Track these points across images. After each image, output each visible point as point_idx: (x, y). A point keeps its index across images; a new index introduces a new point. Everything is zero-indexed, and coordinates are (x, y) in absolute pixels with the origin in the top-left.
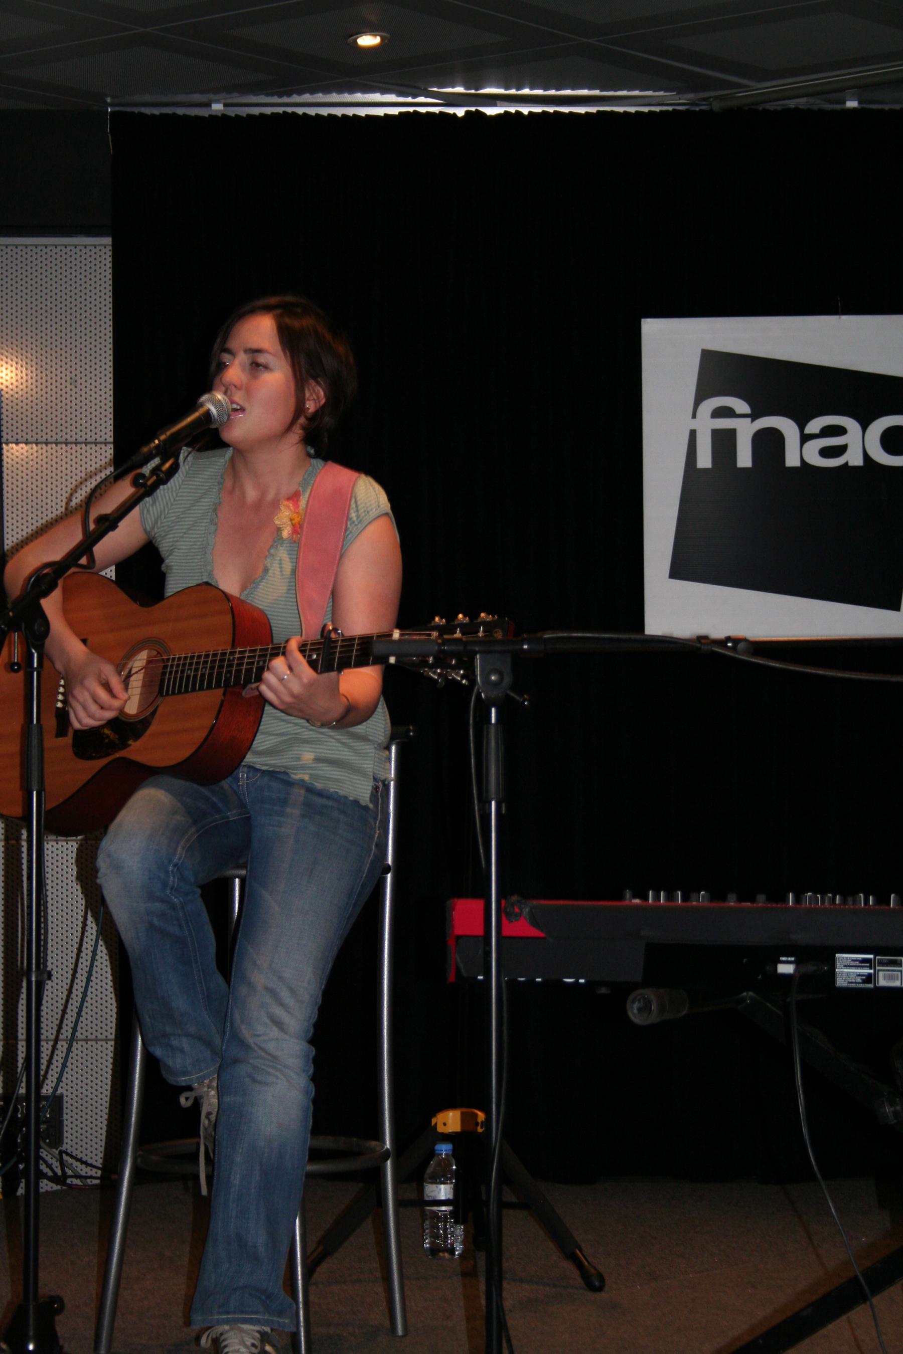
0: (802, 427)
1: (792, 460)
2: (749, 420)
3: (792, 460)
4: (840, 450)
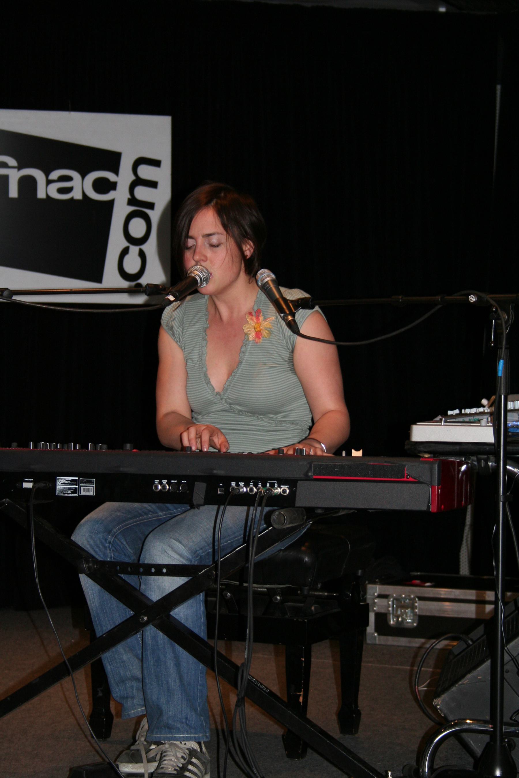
0: (47, 175)
1: (41, 194)
2: (16, 170)
3: (41, 194)
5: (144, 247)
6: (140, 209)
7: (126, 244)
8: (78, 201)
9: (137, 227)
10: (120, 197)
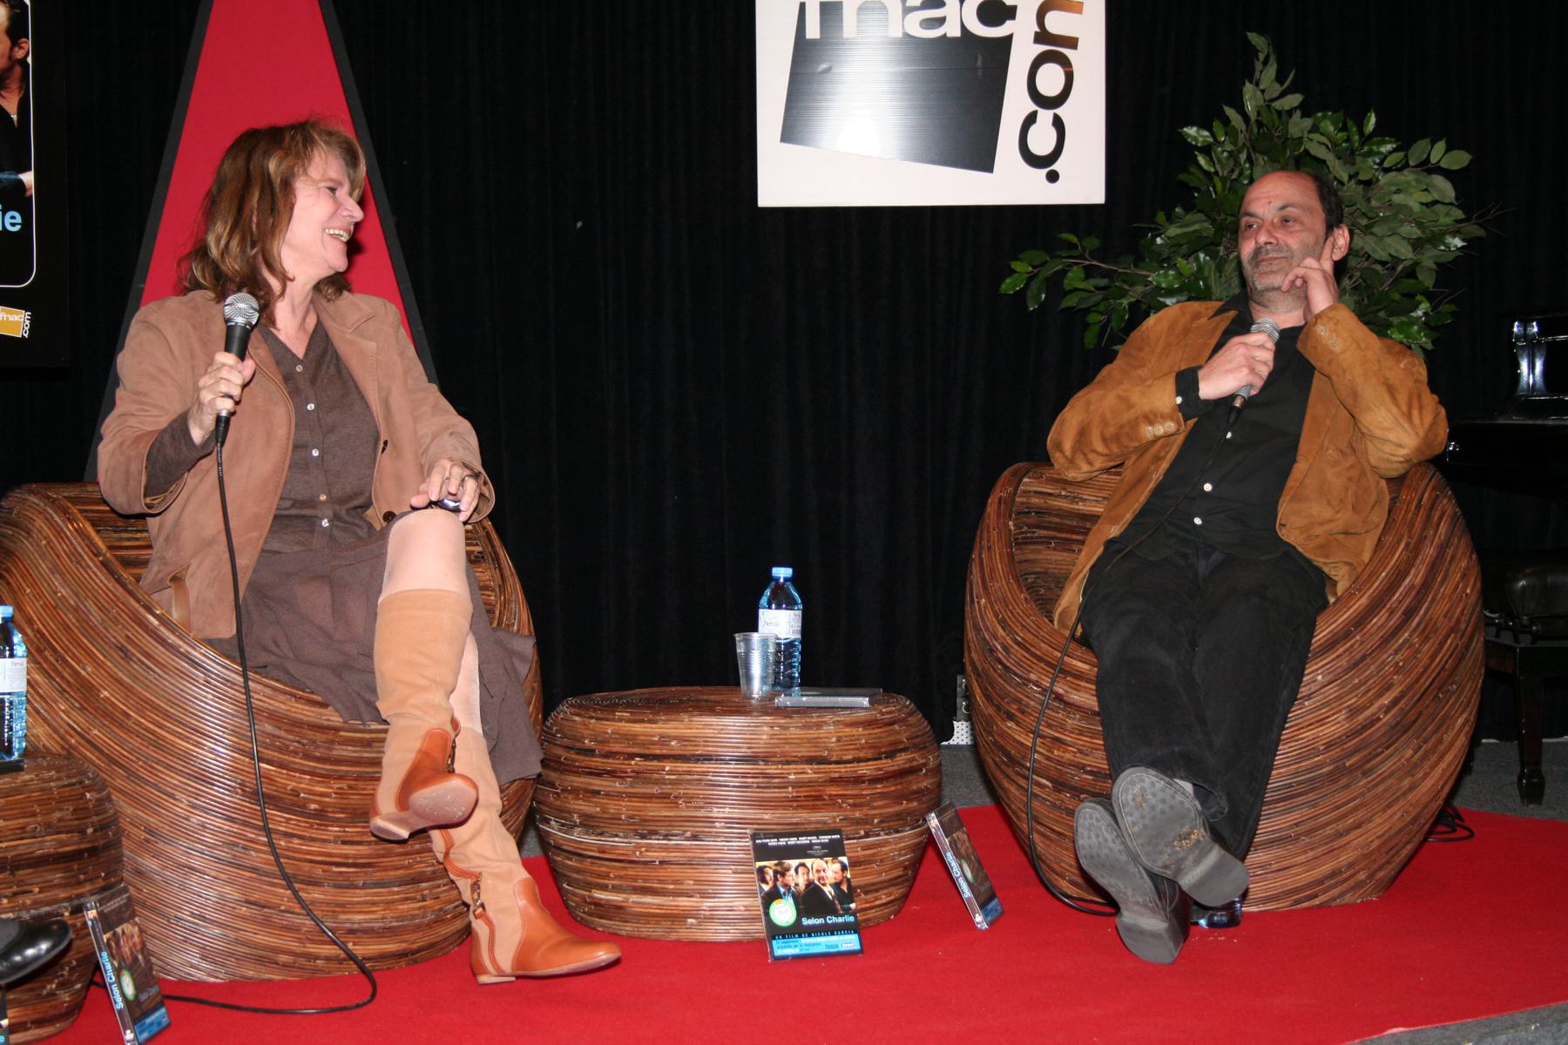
4: (942, 21)
5: (1059, 111)
6: (1054, 49)
7: (1034, 107)
8: (955, 39)
9: (1050, 80)
10: (1021, 30)
